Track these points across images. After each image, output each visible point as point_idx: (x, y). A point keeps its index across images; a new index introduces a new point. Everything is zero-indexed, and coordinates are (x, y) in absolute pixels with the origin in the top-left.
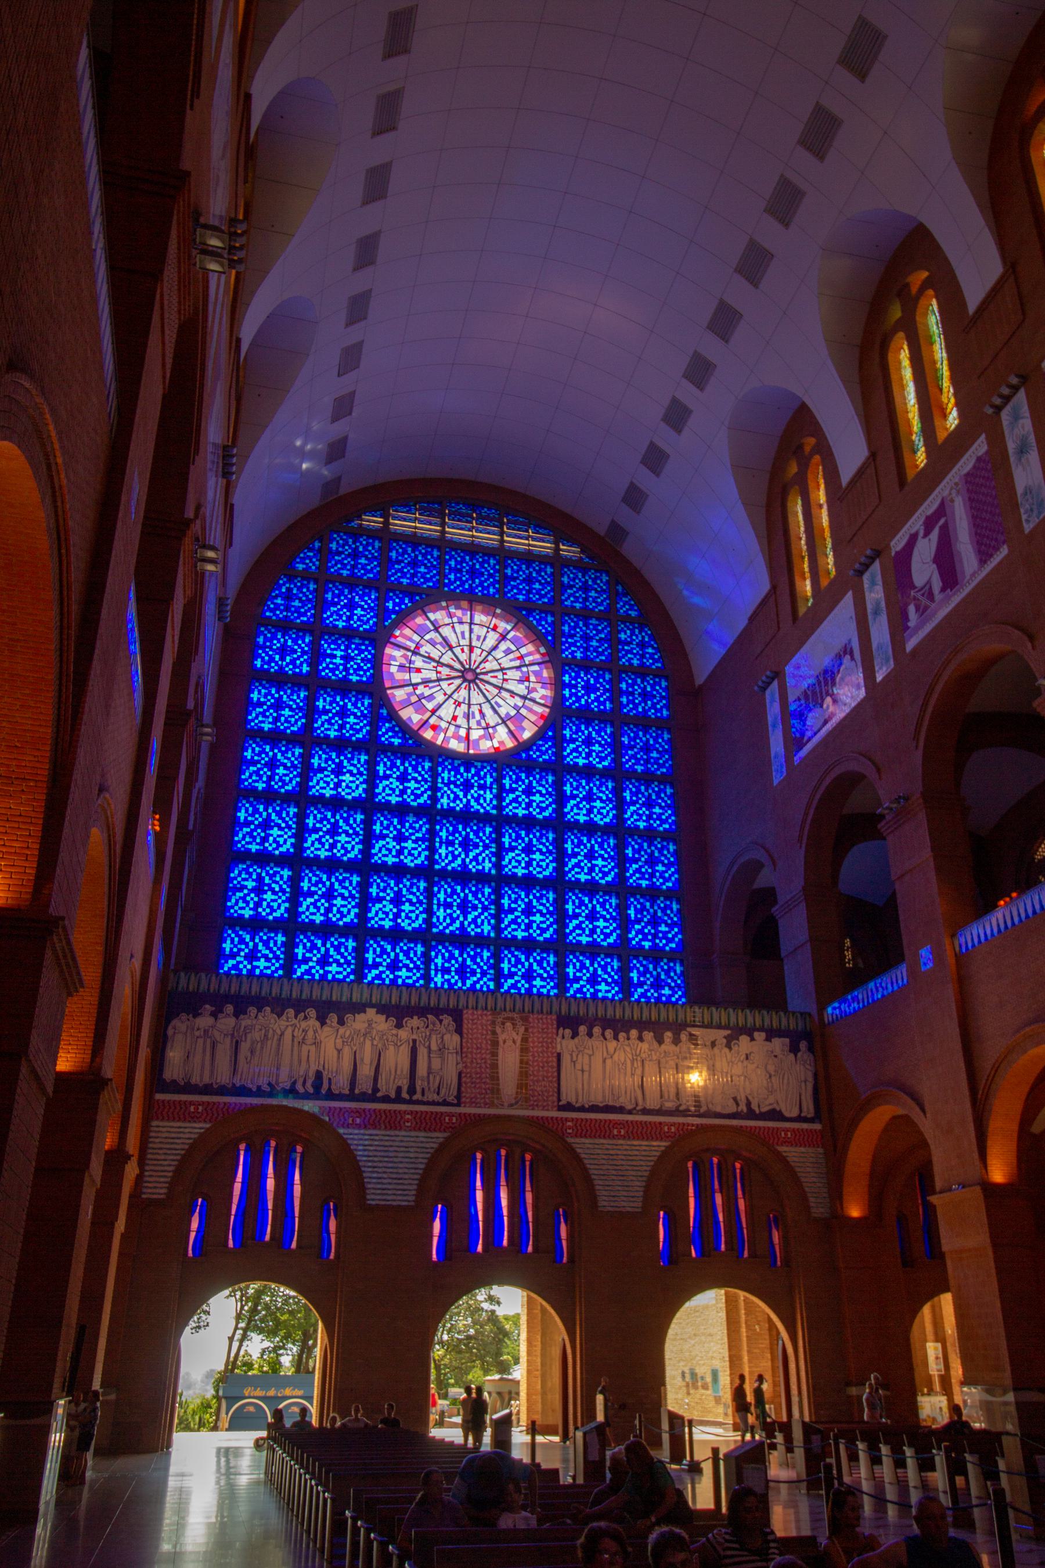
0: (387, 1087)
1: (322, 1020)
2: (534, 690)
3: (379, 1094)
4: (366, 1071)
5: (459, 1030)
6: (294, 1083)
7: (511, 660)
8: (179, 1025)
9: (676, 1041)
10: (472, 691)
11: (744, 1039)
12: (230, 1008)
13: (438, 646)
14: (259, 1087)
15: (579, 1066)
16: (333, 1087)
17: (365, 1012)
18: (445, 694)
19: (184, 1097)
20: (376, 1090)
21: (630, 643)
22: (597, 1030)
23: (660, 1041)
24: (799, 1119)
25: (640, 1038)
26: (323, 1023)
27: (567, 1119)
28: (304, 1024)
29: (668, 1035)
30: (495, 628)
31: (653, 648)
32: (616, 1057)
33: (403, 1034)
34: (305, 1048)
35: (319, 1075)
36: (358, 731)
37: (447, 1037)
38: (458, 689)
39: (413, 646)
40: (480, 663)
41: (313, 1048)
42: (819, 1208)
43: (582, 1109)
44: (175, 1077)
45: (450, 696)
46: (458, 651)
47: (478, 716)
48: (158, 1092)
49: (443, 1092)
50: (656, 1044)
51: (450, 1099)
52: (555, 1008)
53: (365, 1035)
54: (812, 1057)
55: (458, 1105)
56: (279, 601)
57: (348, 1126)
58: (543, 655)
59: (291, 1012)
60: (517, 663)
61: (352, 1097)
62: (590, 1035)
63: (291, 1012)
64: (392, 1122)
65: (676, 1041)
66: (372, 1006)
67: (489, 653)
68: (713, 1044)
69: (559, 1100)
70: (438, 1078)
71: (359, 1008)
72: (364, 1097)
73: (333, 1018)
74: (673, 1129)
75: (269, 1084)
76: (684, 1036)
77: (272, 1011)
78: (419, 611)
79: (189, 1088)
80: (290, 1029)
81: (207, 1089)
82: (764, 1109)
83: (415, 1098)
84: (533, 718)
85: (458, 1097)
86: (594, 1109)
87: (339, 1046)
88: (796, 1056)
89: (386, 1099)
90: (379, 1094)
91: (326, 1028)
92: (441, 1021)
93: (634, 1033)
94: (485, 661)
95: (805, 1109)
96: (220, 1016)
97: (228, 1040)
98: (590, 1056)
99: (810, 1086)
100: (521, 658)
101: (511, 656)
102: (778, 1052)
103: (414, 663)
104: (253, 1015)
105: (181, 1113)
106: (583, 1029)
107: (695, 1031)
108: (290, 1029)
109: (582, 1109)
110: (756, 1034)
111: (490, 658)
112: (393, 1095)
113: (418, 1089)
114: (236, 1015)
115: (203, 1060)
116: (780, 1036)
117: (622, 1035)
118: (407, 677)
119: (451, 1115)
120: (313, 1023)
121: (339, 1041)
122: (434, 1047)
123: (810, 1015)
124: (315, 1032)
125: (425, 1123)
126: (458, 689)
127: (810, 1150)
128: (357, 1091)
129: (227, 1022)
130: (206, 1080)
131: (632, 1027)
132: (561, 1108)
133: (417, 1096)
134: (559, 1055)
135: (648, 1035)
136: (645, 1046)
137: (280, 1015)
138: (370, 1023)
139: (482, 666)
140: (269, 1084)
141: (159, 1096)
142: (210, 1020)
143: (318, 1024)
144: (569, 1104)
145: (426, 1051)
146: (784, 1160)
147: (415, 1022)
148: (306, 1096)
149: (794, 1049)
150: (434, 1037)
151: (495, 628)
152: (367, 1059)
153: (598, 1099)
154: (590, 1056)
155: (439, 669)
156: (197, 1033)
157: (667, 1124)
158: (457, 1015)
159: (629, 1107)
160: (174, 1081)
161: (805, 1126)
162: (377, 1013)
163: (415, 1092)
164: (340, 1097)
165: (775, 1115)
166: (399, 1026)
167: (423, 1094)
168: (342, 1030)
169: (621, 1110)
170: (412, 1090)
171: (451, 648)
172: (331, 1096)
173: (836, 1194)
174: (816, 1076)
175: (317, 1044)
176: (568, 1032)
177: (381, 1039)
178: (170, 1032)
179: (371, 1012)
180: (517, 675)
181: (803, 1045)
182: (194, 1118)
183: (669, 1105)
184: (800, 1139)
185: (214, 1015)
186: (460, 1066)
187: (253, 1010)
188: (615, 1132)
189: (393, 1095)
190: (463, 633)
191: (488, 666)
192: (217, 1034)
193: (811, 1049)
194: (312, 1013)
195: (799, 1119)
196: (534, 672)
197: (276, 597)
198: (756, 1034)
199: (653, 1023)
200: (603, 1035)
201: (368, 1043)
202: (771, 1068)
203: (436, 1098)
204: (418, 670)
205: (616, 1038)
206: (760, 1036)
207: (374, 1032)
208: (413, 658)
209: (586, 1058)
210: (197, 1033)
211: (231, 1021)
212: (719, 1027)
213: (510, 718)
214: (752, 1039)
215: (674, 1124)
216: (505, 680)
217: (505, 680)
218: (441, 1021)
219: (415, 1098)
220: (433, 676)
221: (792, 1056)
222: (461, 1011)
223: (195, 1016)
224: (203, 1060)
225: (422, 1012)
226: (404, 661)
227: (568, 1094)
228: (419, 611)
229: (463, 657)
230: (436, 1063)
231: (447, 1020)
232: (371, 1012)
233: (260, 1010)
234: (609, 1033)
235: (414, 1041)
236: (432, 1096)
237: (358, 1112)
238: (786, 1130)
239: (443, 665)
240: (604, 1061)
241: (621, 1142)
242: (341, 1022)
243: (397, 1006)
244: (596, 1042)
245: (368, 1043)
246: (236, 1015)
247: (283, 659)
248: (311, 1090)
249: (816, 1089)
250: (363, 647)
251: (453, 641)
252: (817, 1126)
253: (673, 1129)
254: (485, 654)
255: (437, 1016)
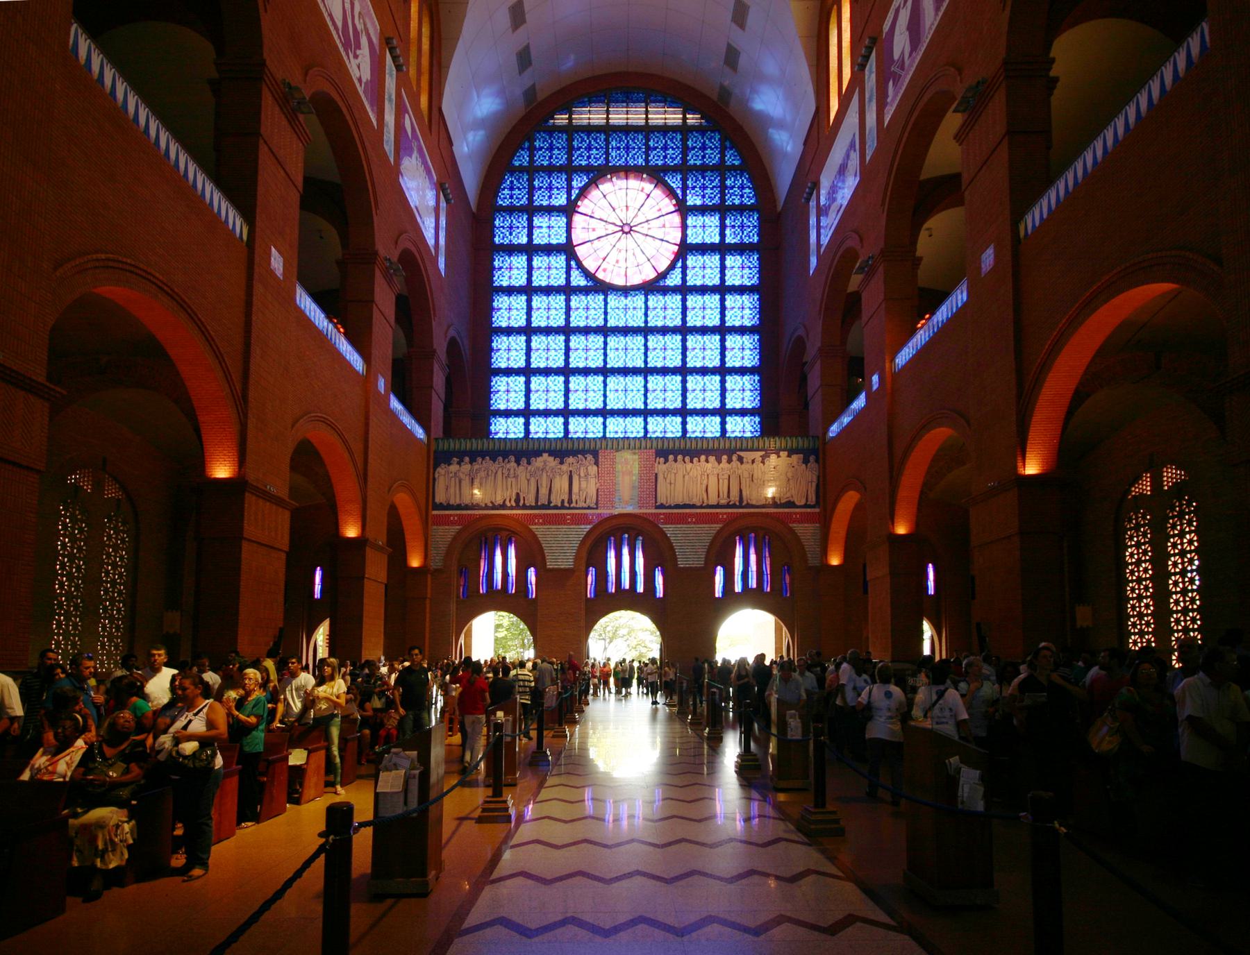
0: (556, 501)
1: (518, 462)
2: (668, 233)
3: (552, 505)
4: (544, 491)
5: (597, 463)
6: (505, 500)
8: (441, 470)
9: (730, 461)
11: (773, 457)
12: (467, 459)
14: (486, 504)
15: (668, 481)
16: (526, 502)
17: (542, 455)
19: (447, 512)
20: (550, 502)
21: (734, 187)
22: (680, 457)
23: (719, 462)
24: (806, 506)
25: (707, 461)
26: (519, 464)
27: (660, 514)
28: (508, 466)
29: (725, 458)
30: (642, 190)
31: (750, 188)
32: (691, 474)
33: (564, 467)
34: (509, 480)
35: (518, 495)
37: (589, 468)
41: (514, 480)
42: (813, 561)
43: (670, 507)
44: (441, 501)
48: (433, 509)
49: (587, 502)
50: (716, 463)
51: (592, 505)
52: (654, 445)
53: (542, 470)
54: (817, 465)
55: (597, 508)
56: (506, 192)
57: (535, 524)
58: (674, 205)
59: (500, 459)
61: (536, 507)
62: (676, 460)
63: (500, 459)
64: (559, 520)
65: (730, 461)
66: (545, 451)
67: (639, 210)
68: (753, 462)
69: (656, 502)
70: (585, 493)
71: (538, 453)
72: (543, 507)
73: (524, 461)
74: (725, 516)
75: (492, 502)
76: (734, 458)
77: (490, 459)
78: (594, 185)
79: (449, 507)
80: (501, 469)
81: (459, 507)
82: (783, 501)
83: (572, 506)
85: (597, 503)
86: (677, 506)
87: (528, 477)
88: (806, 465)
89: (556, 507)
90: (552, 505)
91: (520, 467)
92: (586, 458)
93: (703, 458)
94: (636, 215)
95: (809, 500)
96: (462, 464)
97: (467, 478)
98: (675, 474)
99: (814, 485)
100: (660, 210)
102: (795, 463)
104: (480, 462)
105: (444, 521)
106: (671, 457)
107: (742, 454)
108: (501, 469)
109: (670, 507)
110: (781, 453)
112: (559, 505)
113: (574, 500)
114: (471, 463)
115: (455, 491)
116: (797, 454)
117: (695, 460)
119: (593, 515)
120: (513, 464)
121: (528, 474)
122: (582, 475)
123: (818, 437)
124: (515, 470)
125: (579, 520)
127: (810, 525)
128: (539, 504)
129: (466, 467)
130: (458, 502)
131: (702, 454)
132: (657, 507)
133: (573, 505)
134: (656, 474)
135: (712, 459)
136: (709, 465)
137: (494, 461)
138: (545, 462)
140: (492, 502)
141: (435, 512)
142: (457, 467)
143: (516, 465)
144: (662, 504)
145: (577, 477)
146: (792, 531)
147: (571, 460)
148: (512, 508)
149: (806, 461)
150: (582, 468)
151: (642, 190)
152: (544, 485)
153: (679, 501)
154: (675, 474)
156: (451, 475)
157: (721, 514)
158: (595, 454)
159: (699, 504)
160: (441, 503)
161: (809, 510)
162: (549, 455)
163: (572, 502)
164: (531, 508)
165: (790, 504)
166: (562, 463)
167: (577, 503)
168: (529, 468)
169: (693, 506)
170: (570, 501)
172: (525, 507)
173: (825, 553)
174: (819, 477)
175: (516, 477)
176: (662, 460)
177: (552, 472)
178: (436, 476)
179: (545, 455)
181: (812, 458)
182: (453, 523)
183: (723, 502)
184: (805, 518)
185: (459, 463)
186: (598, 485)
187: (479, 459)
188: (690, 520)
189: (559, 505)
192: (461, 475)
193: (817, 461)
194: (513, 458)
195: (806, 506)
197: (503, 190)
198: (781, 453)
199: (716, 450)
200: (684, 460)
201: (544, 474)
202: (790, 475)
203: (585, 505)
204: (594, 230)
205: (692, 461)
206: (784, 454)
207: (548, 468)
209: (673, 475)
210: (451, 475)
211: (469, 466)
212: (758, 450)
214: (779, 456)
215: (726, 513)
216: (649, 229)
217: (649, 229)
218: (586, 458)
219: (572, 506)
221: (804, 465)
222: (598, 451)
223: (449, 465)
224: (455, 491)
225: (574, 453)
227: (662, 499)
228: (594, 185)
229: (622, 216)
230: (584, 484)
231: (590, 457)
232: (545, 455)
233: (483, 459)
234: (687, 459)
235: (571, 471)
236: (581, 504)
237: (540, 516)
238: (796, 514)
240: (684, 477)
241: (692, 526)
242: (529, 463)
243: (560, 451)
244: (680, 465)
245: (544, 474)
246: (471, 463)
247: (511, 234)
248: (514, 504)
249: (818, 486)
252: (817, 510)
253: (725, 516)
255: (583, 455)
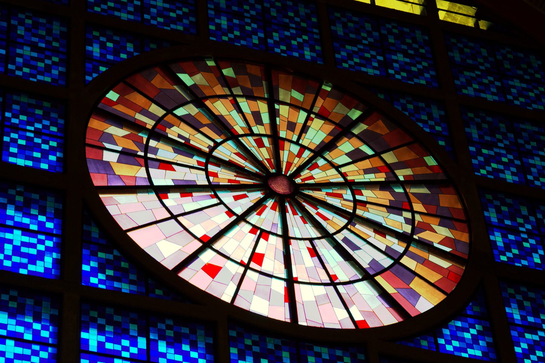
7: (367, 171)
10: (289, 215)
13: (205, 130)
18: (230, 213)
36: (33, 259)
38: (258, 207)
39: (150, 123)
40: (301, 168)
45: (242, 218)
46: (249, 142)
47: (310, 262)
60: (381, 177)
84: (434, 277)
101: (366, 164)
103: (155, 150)
111: (321, 162)
118: (142, 172)
126: (258, 207)
139: (305, 173)
155: (212, 168)
171: (233, 136)
180: (385, 197)
190: (257, 116)
191: (318, 175)
196: (421, 197)
204: (167, 165)
208: (153, 143)
213: (382, 271)
217: (356, 203)
220: (201, 179)
226: (132, 146)
239: (220, 162)
250: (39, 112)
251: (239, 126)
254: (307, 154)
